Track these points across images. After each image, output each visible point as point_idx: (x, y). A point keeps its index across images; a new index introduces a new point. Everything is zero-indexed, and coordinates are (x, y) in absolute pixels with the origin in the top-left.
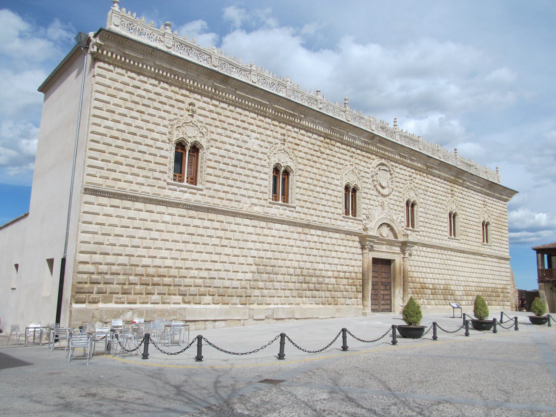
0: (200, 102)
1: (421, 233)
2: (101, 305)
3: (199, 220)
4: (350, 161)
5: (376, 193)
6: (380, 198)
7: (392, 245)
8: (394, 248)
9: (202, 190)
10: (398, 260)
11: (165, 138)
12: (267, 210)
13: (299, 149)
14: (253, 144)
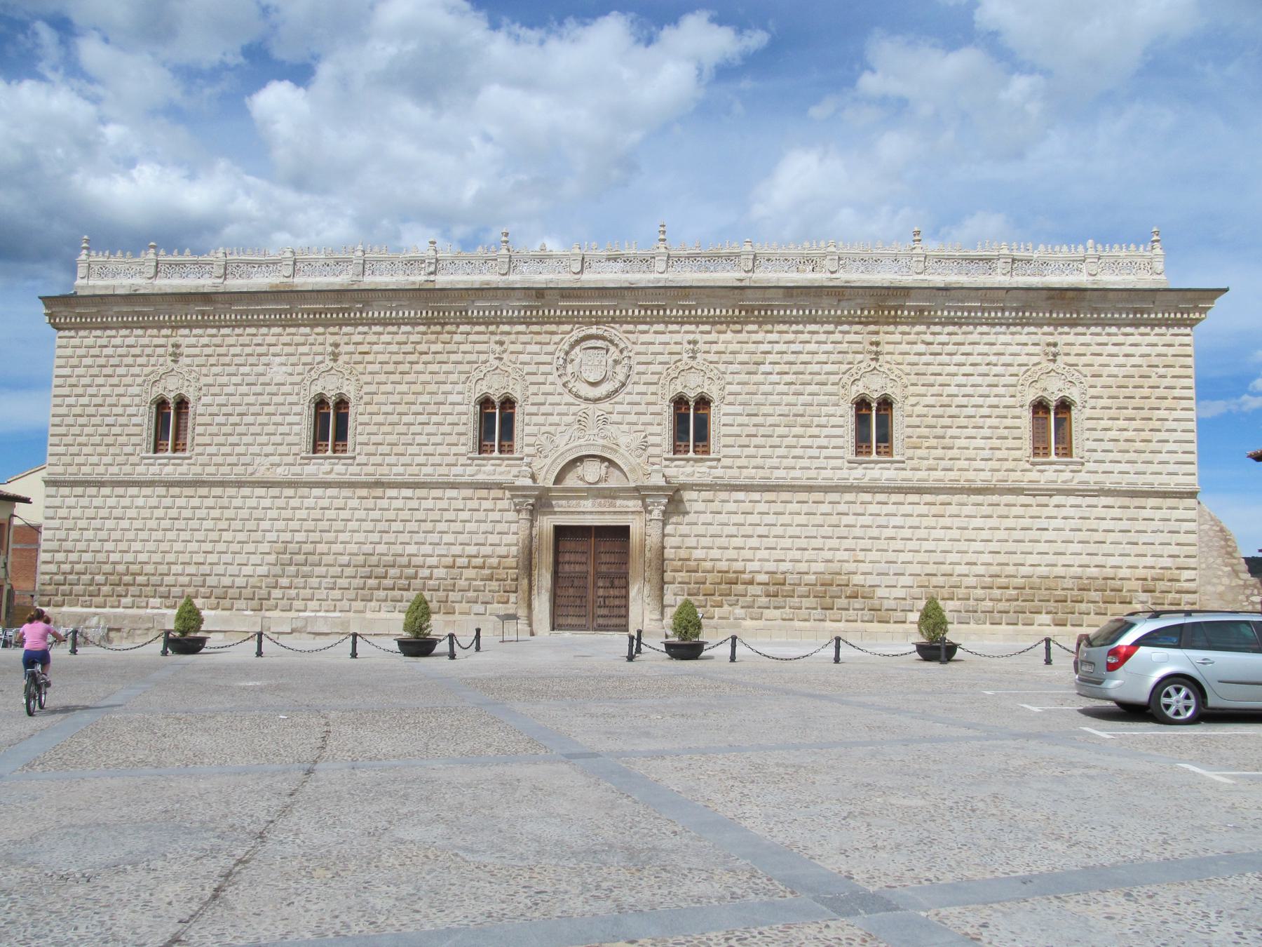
0: (185, 338)
1: (725, 462)
2: (65, 609)
3: (183, 500)
4: (494, 352)
5: (571, 399)
6: (583, 406)
7: (614, 498)
8: (619, 502)
9: (190, 458)
10: (636, 527)
11: (137, 400)
12: (297, 469)
13: (362, 365)
14: (278, 373)
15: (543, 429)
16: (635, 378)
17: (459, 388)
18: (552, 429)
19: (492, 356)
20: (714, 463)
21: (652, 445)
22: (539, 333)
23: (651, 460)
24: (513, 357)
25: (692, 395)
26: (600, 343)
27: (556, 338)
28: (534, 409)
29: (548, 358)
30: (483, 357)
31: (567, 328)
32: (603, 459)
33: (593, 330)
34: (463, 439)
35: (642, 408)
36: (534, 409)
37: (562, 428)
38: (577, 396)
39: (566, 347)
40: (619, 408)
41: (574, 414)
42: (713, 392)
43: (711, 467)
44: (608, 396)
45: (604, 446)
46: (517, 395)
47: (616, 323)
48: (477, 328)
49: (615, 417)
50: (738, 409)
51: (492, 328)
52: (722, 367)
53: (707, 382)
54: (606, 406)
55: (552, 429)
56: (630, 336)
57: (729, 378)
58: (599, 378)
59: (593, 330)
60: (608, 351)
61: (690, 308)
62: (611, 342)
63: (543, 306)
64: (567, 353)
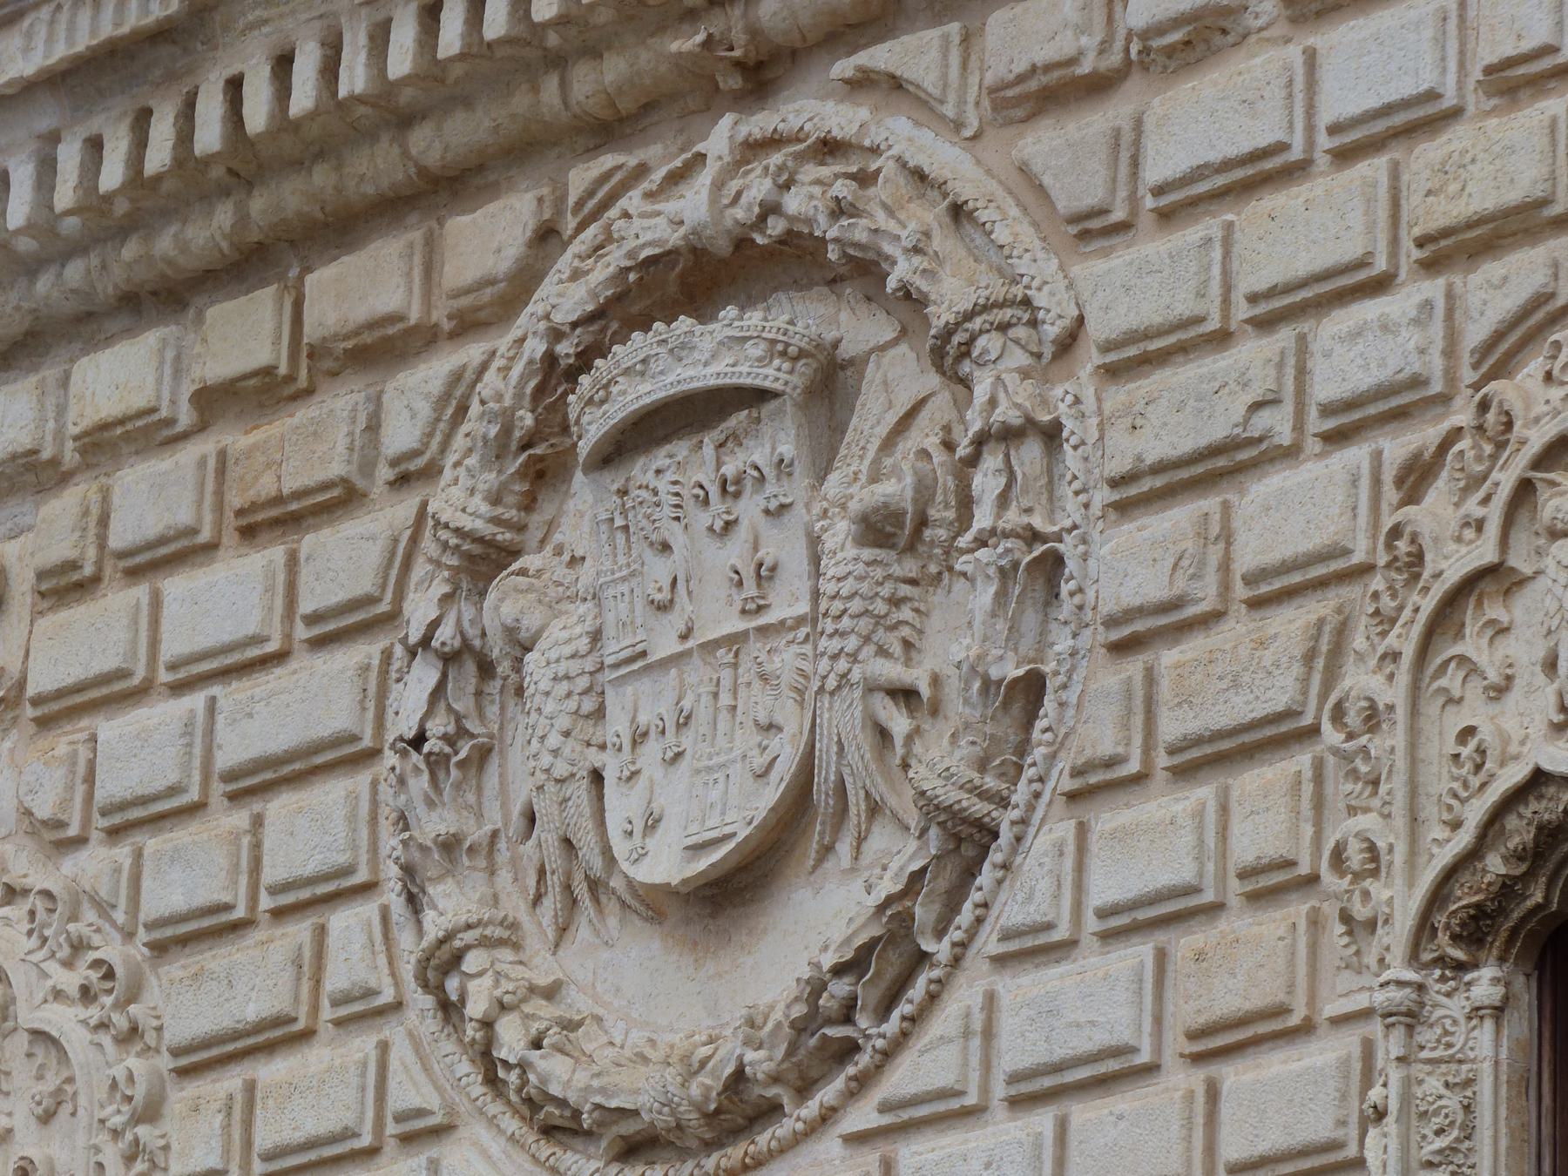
16: (1093, 712)
58: (744, 809)
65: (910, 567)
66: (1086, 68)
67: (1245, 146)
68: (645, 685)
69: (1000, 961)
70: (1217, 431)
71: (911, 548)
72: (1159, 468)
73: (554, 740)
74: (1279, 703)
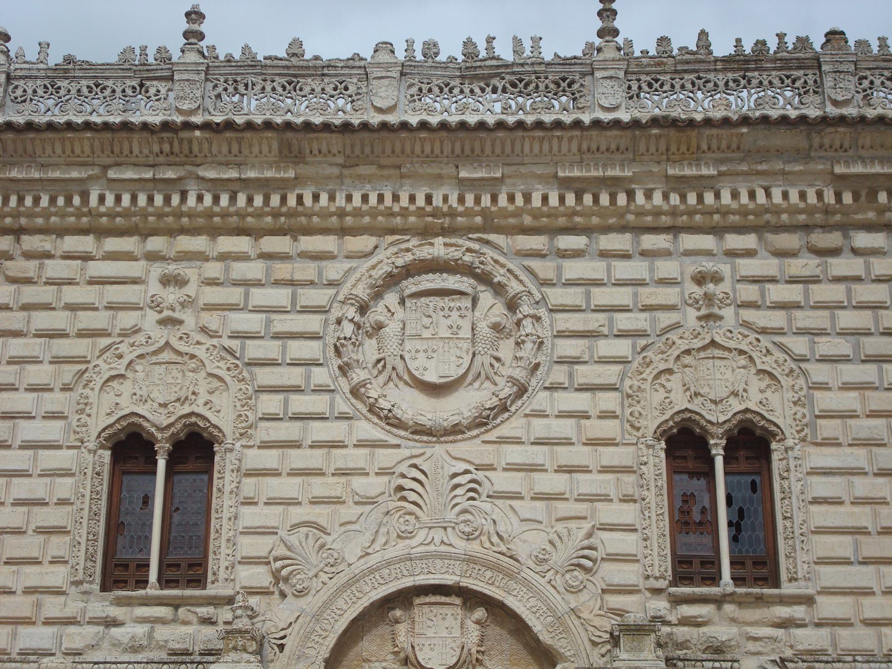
4: (156, 306)
15: (298, 514)
17: (55, 401)
18: (320, 514)
19: (152, 316)
20: (798, 612)
21: (613, 558)
22: (284, 257)
23: (615, 601)
24: (212, 320)
25: (718, 417)
26: (452, 282)
27: (333, 270)
28: (269, 458)
29: (313, 323)
30: (127, 319)
31: (364, 242)
32: (470, 598)
33: (438, 248)
34: (58, 545)
35: (578, 455)
36: (269, 458)
37: (349, 512)
38: (392, 421)
39: (362, 292)
40: (515, 454)
41: (383, 472)
42: (779, 409)
43: (785, 624)
44: (482, 422)
45: (470, 560)
46: (222, 414)
47: (499, 230)
48: (113, 244)
49: (502, 481)
50: (858, 457)
51: (156, 243)
52: (799, 345)
53: (756, 384)
54: (471, 448)
55: (320, 514)
56: (535, 264)
57: (819, 372)
58: (455, 372)
59: (438, 248)
60: (475, 301)
61: (700, 184)
62: (485, 279)
63: (297, 181)
64: (363, 309)
65: (498, 335)
66: (544, 252)
67: (594, 277)
68: (419, 341)
69: (526, 415)
70: (591, 328)
71: (498, 332)
72: (570, 332)
73: (394, 347)
74: (613, 382)
